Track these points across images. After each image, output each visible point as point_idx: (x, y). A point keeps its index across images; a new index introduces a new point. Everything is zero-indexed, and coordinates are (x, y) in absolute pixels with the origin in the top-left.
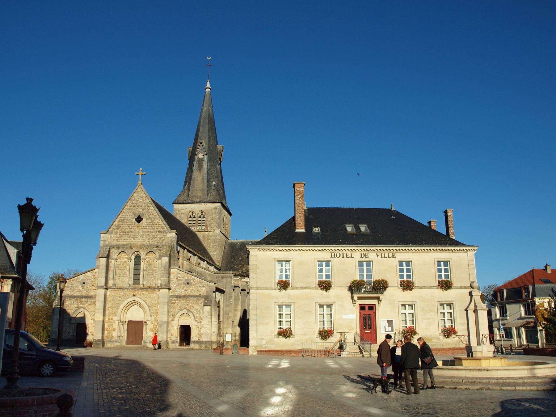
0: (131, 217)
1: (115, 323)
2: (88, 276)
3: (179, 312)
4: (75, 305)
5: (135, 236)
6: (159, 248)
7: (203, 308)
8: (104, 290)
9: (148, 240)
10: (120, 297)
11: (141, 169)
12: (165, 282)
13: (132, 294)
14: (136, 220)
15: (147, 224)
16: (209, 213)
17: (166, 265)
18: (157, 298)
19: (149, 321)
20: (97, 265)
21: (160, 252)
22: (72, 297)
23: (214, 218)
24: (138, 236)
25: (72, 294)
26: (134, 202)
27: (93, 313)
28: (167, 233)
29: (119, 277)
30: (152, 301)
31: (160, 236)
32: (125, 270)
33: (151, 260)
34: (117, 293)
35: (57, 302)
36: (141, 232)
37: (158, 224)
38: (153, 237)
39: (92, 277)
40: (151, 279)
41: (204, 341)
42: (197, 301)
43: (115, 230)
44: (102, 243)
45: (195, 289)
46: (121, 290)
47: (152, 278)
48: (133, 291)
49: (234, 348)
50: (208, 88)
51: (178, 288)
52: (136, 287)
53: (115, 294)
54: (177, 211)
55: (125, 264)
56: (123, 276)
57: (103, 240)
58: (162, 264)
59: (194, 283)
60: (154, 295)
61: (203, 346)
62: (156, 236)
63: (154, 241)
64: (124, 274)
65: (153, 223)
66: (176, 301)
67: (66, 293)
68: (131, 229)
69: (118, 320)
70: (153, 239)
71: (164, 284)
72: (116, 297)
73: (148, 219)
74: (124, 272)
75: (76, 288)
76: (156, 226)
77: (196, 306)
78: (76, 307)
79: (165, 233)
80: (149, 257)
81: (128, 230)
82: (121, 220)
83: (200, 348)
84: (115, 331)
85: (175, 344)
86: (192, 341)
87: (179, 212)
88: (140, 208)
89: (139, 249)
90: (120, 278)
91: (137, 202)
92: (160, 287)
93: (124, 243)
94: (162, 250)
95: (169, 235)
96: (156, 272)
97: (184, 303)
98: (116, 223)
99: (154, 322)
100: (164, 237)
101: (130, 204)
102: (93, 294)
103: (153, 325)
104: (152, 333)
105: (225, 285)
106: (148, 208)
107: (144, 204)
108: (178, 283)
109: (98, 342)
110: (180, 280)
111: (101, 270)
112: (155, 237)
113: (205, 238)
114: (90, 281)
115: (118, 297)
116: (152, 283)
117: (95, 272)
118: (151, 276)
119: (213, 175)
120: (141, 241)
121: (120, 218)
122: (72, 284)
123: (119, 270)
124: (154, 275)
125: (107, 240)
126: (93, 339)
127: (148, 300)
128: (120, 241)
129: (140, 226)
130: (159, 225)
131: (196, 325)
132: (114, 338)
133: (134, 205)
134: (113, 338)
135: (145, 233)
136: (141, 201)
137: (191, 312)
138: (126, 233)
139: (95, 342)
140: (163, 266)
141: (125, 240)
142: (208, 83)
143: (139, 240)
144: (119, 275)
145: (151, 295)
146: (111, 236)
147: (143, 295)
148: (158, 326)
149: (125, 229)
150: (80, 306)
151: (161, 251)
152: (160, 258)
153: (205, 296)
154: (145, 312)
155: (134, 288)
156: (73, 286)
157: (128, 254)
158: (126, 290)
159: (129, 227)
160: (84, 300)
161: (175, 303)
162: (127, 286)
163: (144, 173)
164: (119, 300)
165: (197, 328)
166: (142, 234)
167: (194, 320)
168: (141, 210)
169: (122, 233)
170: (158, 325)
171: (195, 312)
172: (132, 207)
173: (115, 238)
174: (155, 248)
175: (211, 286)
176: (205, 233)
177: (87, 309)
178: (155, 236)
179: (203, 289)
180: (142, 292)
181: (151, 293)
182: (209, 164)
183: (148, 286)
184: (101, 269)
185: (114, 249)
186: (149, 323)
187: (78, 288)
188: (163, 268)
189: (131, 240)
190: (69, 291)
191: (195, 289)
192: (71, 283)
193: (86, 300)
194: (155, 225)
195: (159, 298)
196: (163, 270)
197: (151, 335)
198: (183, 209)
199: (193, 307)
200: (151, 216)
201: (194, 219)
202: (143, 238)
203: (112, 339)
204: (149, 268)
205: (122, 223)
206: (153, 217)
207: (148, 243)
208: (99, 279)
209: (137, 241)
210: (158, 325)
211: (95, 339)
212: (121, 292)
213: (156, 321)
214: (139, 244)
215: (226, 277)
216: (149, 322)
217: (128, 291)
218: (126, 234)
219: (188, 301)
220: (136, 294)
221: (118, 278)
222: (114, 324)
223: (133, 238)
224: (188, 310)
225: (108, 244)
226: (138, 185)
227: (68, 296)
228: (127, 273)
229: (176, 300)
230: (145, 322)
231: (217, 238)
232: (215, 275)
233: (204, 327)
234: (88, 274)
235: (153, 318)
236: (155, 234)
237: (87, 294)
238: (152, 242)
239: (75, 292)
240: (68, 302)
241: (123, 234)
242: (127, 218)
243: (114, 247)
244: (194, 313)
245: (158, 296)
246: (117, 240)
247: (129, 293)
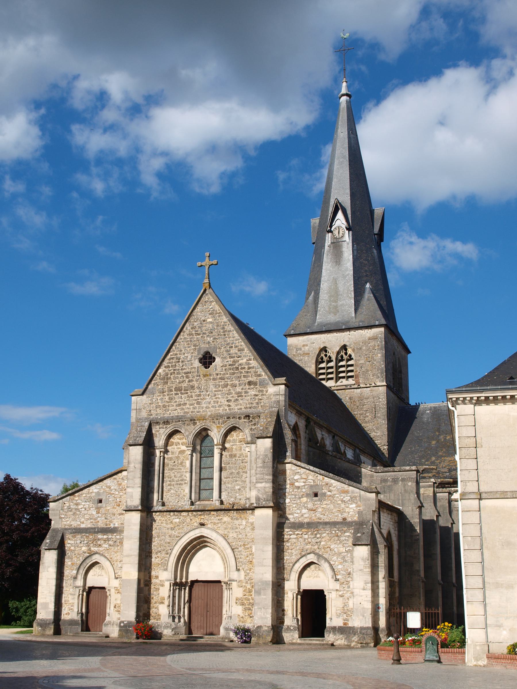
0: (192, 356)
1: (163, 585)
2: (108, 485)
3: (298, 560)
4: (84, 549)
5: (200, 395)
6: (251, 419)
7: (350, 552)
8: (139, 515)
9: (227, 403)
10: (172, 529)
11: (207, 254)
12: (266, 492)
13: (196, 521)
14: (201, 363)
15: (224, 368)
16: (361, 348)
17: (267, 455)
18: (248, 529)
19: (233, 581)
20: (125, 461)
21: (253, 427)
22: (78, 531)
23: (372, 357)
24: (206, 395)
25: (79, 525)
26: (196, 323)
27: (120, 565)
28: (268, 384)
29: (169, 485)
30: (240, 536)
31: (252, 392)
32: (181, 469)
33: (234, 447)
34: (166, 520)
35: (48, 541)
36: (212, 388)
37: (246, 367)
38: (238, 396)
40: (237, 487)
41: (358, 628)
42: (337, 536)
43: (160, 387)
44: (133, 414)
45: (332, 506)
46: (174, 515)
47: (238, 485)
48: (200, 515)
49: (428, 647)
50: (343, 95)
51: (294, 506)
52: (205, 506)
53: (162, 523)
54: (295, 350)
55: (182, 458)
56: (177, 484)
58: (258, 453)
59: (329, 493)
60: (244, 522)
61: (355, 638)
62: (243, 394)
63: (241, 405)
64: (180, 479)
65: (237, 365)
66: (290, 535)
67: (65, 523)
68: (192, 381)
69: (170, 580)
70: (237, 400)
71: (264, 497)
72: (165, 530)
73: (225, 358)
74: (179, 475)
75: (86, 512)
76: (243, 371)
77: (336, 546)
78: (85, 552)
79: (263, 385)
80: (231, 439)
81: (186, 385)
82: (170, 365)
83: (347, 645)
84: (163, 603)
85: (292, 634)
86: (329, 627)
87: (298, 352)
88: (208, 336)
89: (208, 424)
90: (172, 487)
91: (201, 323)
92: (255, 505)
93: (179, 412)
94: (258, 422)
95: (272, 390)
96: (246, 473)
97: (310, 540)
98: (160, 371)
99: (244, 584)
100: (261, 394)
101: (189, 328)
102: (118, 524)
104: (241, 607)
105: (401, 497)
106: (225, 335)
107: (218, 326)
108: (295, 495)
109: (129, 627)
110: (298, 488)
111: (132, 472)
112: (242, 396)
113: (354, 401)
114: (113, 495)
115: (168, 529)
116: (240, 495)
117: (121, 477)
118: (236, 481)
119: (366, 268)
120: (213, 407)
121: (170, 359)
122: (77, 504)
123: (169, 470)
124: (243, 478)
125: (144, 409)
126: (119, 621)
127: (232, 535)
128: (170, 408)
129: (210, 375)
130: (249, 368)
131: (337, 590)
132: (161, 619)
133: (197, 331)
134: (160, 618)
135: (220, 388)
137: (326, 560)
138: (181, 390)
139: (123, 626)
140: (261, 457)
141: (180, 405)
142: (344, 84)
143: (210, 403)
144: (170, 481)
145: (236, 522)
146: (151, 400)
147: (219, 525)
148: (253, 593)
149: (179, 383)
150: (92, 549)
151: (255, 424)
152: (253, 442)
153: (355, 522)
154: (224, 559)
155: (200, 509)
156: (80, 507)
157: (188, 436)
158: (184, 514)
159: (187, 377)
160: (100, 536)
161: (290, 539)
162: (186, 505)
163: (215, 262)
164: (170, 536)
165: (341, 596)
166: (215, 391)
167: (333, 578)
168: (211, 339)
169: (174, 392)
170: (253, 590)
171: (335, 560)
172: (192, 334)
173: (160, 404)
174: (243, 420)
175: (369, 499)
176: (354, 392)
178: (241, 393)
179: (351, 506)
180: (218, 518)
181: (237, 519)
182: (355, 248)
183: (231, 503)
184: (132, 470)
185: (158, 427)
186: (234, 584)
187: (90, 512)
188: (260, 461)
189: (191, 405)
190: (71, 519)
191: (332, 506)
192: (75, 502)
193: (105, 537)
194: (242, 369)
195: (253, 529)
196: (261, 467)
197: (240, 614)
198: (307, 345)
199: (329, 549)
200: (231, 352)
202: (216, 398)
203: (157, 620)
204: (231, 464)
205: (172, 371)
206: (236, 353)
207: (227, 408)
208: (129, 490)
209: (205, 406)
210: (253, 590)
211: (123, 620)
212: (174, 517)
213: (249, 582)
214: (209, 414)
215: (403, 480)
216: (233, 582)
217: (188, 515)
218: (182, 394)
219: (318, 536)
220: (206, 521)
221: (169, 487)
222: (161, 588)
223: (196, 400)
224: (319, 556)
225: (146, 416)
226: (203, 289)
227: (69, 529)
228: (185, 476)
229: (291, 533)
230: (226, 583)
231: (381, 400)
232: (377, 476)
233: (357, 595)
234: (108, 482)
235: (242, 573)
236: (242, 389)
238: (235, 408)
239: (83, 520)
240: (69, 542)
241: (176, 394)
242: (182, 359)
243: (157, 423)
244: (332, 563)
245: (252, 524)
246: (164, 406)
247: (191, 520)
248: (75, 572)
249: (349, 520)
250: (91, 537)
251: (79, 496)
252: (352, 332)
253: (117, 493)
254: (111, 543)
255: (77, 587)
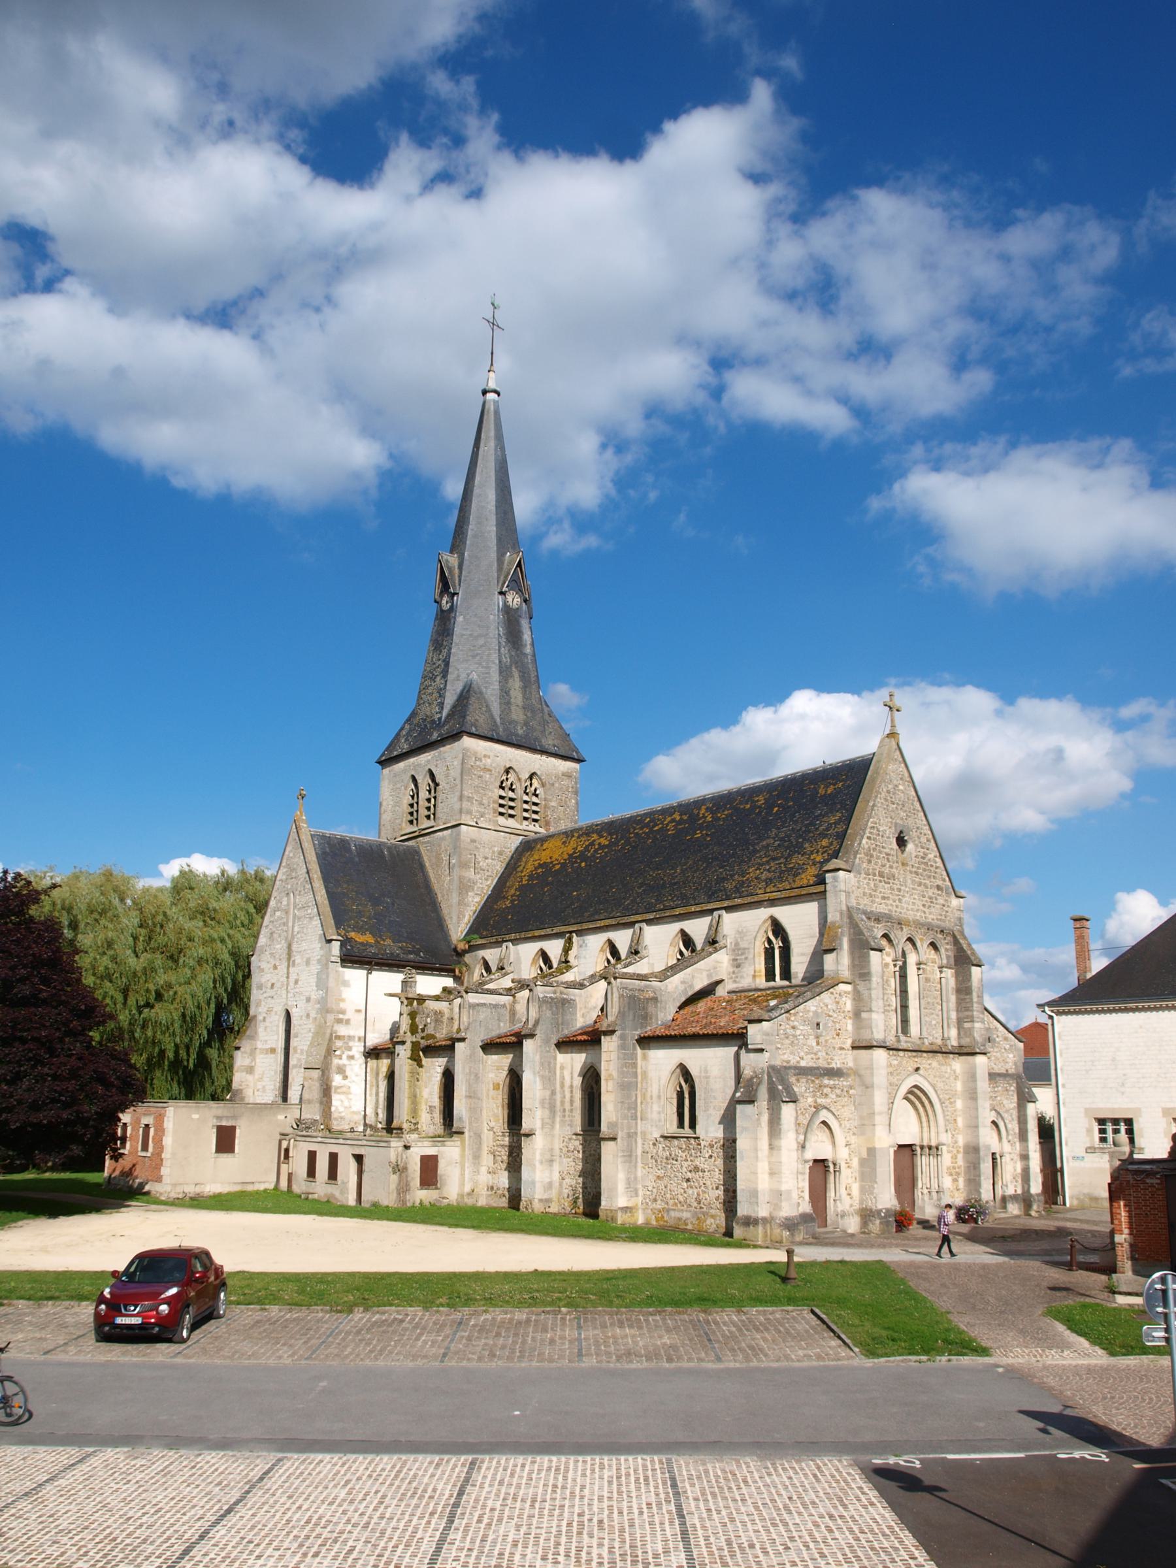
2: (826, 1001)
18: (952, 1078)
22: (802, 1072)
25: (798, 1062)
30: (946, 1087)
39: (834, 1008)
40: (934, 1022)
57: (845, 891)
78: (810, 1106)
87: (478, 763)
93: (882, 908)
103: (950, 1155)
122: (793, 1028)
127: (940, 1085)
136: (901, 787)
141: (884, 898)
145: (943, 1068)
146: (859, 882)
150: (819, 1101)
156: (798, 1032)
158: (901, 1053)
160: (826, 1081)
173: (866, 891)
177: (833, 1110)
192: (791, 1023)
193: (832, 1082)
201: (511, 794)
237: (829, 1064)
239: (802, 1054)
241: (880, 881)
248: (802, 1137)
249: (1010, 1072)
250: (817, 1082)
251: (795, 1015)
252: (544, 757)
253: (835, 1015)
254: (838, 1091)
255: (806, 1161)
